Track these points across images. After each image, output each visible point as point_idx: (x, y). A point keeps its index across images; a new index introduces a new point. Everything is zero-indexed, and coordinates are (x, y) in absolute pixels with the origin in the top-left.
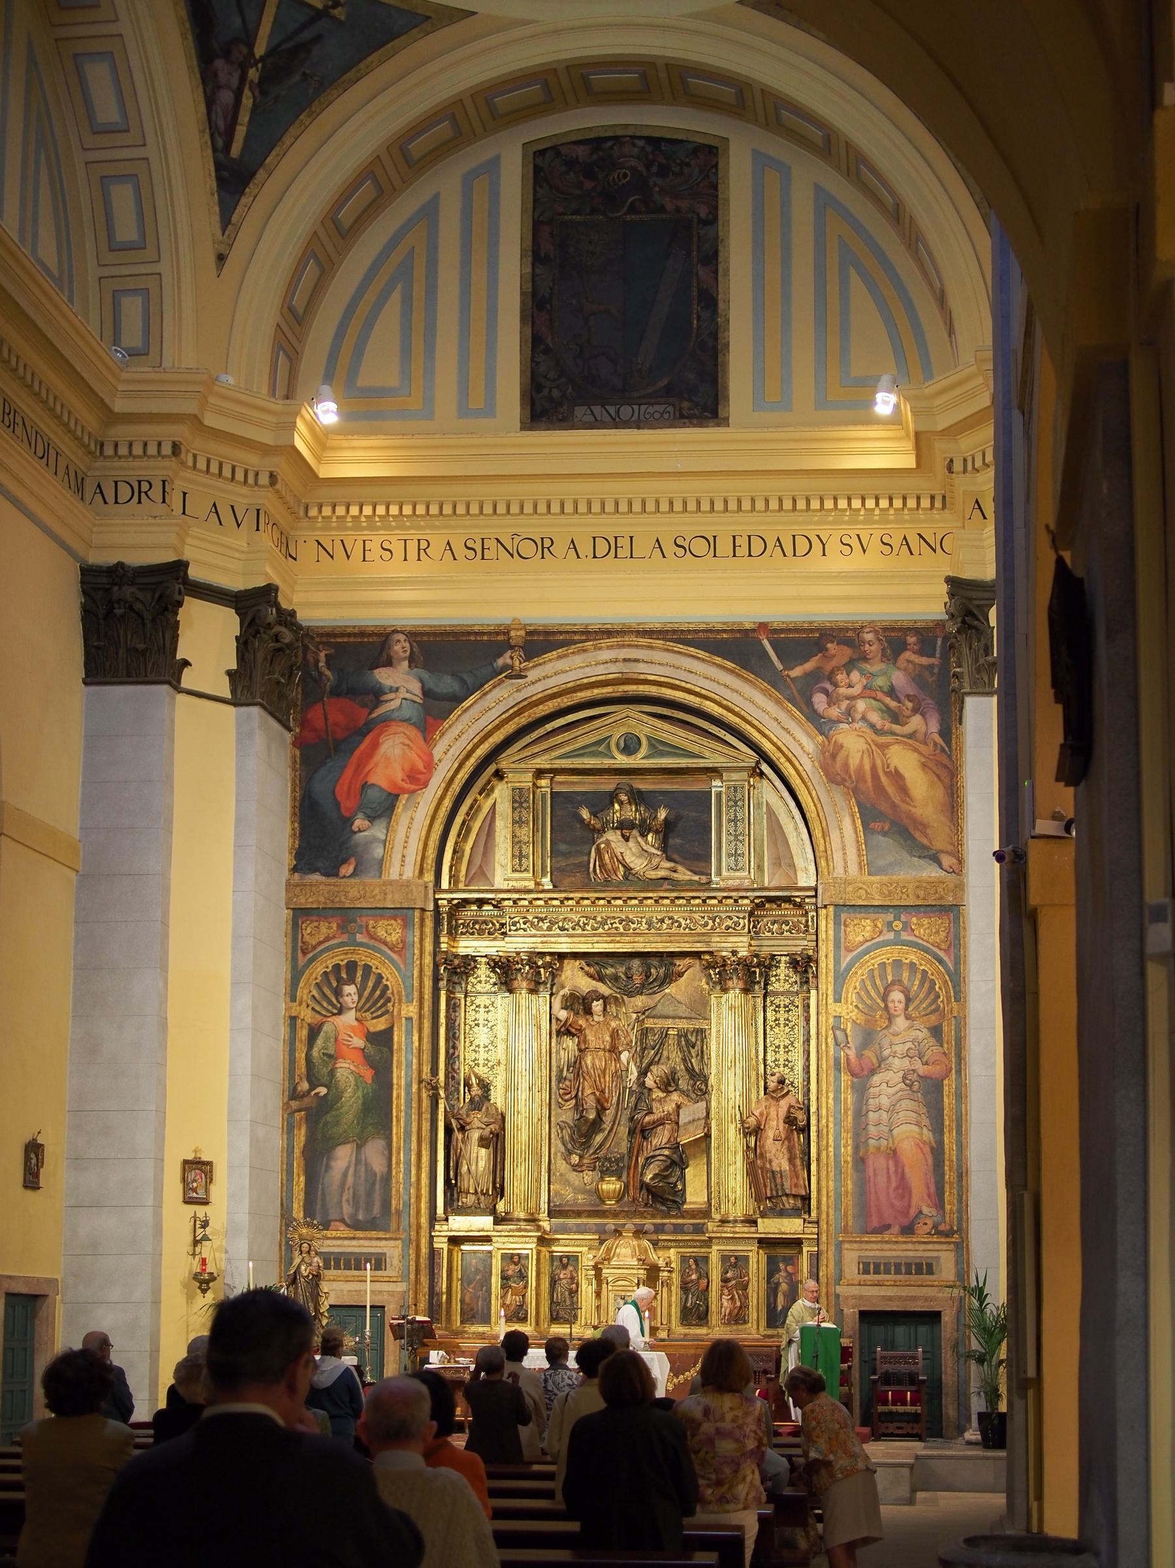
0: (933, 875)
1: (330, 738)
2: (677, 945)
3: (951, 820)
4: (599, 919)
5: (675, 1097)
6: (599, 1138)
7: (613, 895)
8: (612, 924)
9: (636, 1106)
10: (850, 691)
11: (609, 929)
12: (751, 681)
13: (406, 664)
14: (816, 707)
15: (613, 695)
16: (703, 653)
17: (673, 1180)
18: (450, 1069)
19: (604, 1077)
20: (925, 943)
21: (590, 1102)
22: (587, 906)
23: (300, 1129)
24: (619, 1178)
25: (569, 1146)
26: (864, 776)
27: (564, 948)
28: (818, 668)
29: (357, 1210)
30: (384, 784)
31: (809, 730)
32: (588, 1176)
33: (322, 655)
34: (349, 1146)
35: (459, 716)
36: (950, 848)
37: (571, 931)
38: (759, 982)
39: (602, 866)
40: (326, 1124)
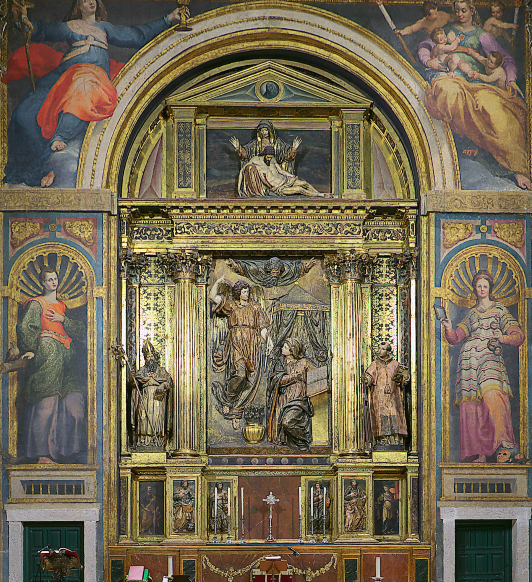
0: (511, 190)
1: (32, 76)
2: (308, 245)
3: (525, 149)
4: (246, 225)
5: (303, 362)
6: (245, 393)
7: (260, 204)
8: (257, 229)
9: (274, 369)
10: (448, 47)
11: (255, 233)
12: (371, 37)
13: (94, 16)
14: (421, 59)
15: (260, 47)
16: (332, 14)
17: (304, 424)
18: (128, 342)
19: (250, 347)
20: (505, 243)
21: (241, 365)
22: (238, 215)
23: (13, 385)
24: (261, 424)
25: (222, 400)
26: (458, 114)
27: (218, 247)
28: (423, 29)
29: (60, 447)
30: (77, 113)
31: (416, 76)
32: (237, 423)
33: (24, 8)
34: (52, 398)
35: (138, 59)
36: (524, 170)
37: (225, 234)
38: (368, 276)
39: (250, 184)
40: (33, 382)
